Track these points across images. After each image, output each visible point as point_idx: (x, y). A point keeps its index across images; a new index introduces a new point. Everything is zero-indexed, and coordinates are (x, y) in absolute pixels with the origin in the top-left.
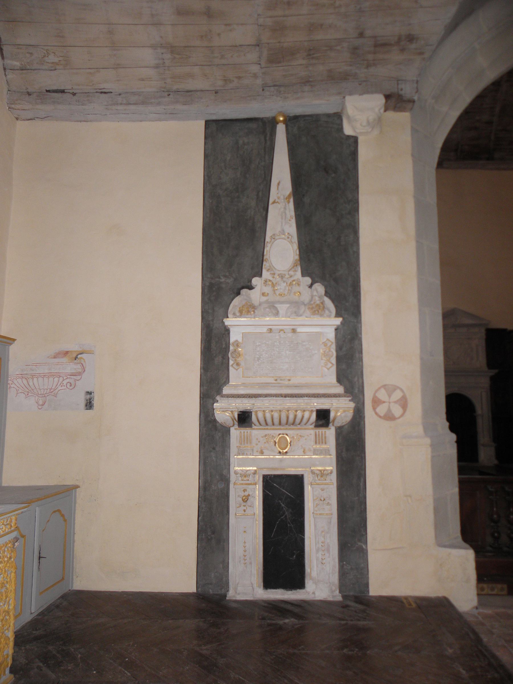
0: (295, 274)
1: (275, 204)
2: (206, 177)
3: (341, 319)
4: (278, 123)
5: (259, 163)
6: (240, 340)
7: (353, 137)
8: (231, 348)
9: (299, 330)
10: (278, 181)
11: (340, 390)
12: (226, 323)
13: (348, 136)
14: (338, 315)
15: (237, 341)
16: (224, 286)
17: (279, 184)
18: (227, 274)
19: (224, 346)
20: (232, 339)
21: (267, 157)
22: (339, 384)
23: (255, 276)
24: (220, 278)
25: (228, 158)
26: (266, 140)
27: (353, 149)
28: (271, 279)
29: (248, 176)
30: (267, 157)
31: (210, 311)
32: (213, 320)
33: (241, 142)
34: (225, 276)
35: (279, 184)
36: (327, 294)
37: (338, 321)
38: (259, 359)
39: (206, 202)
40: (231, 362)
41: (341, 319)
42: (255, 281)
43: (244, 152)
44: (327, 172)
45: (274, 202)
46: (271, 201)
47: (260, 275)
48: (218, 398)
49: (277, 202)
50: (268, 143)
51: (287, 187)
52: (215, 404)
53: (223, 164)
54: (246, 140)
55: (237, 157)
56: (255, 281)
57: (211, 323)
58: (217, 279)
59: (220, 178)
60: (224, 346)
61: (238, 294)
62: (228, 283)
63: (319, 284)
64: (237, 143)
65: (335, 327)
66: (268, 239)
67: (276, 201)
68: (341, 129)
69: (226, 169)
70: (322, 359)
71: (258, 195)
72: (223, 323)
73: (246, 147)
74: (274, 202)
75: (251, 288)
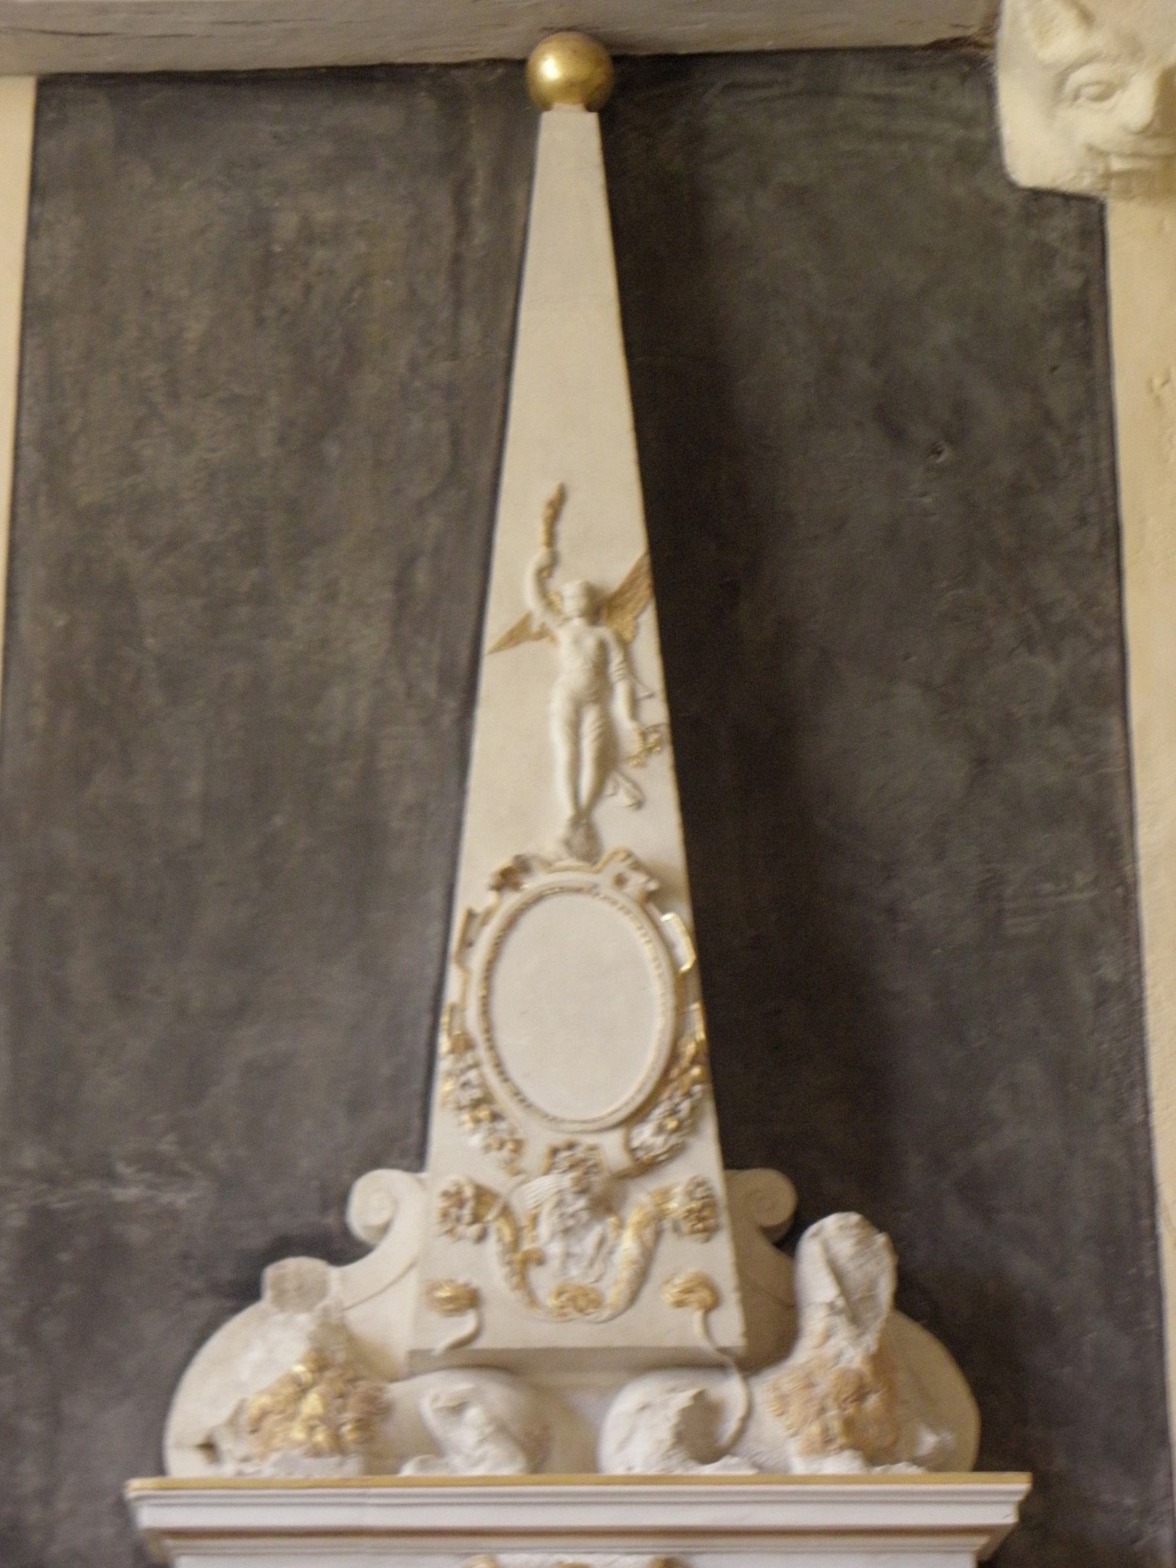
0: (675, 1152)
1: (526, 649)
2: (32, 457)
3: (1019, 1484)
4: (547, 107)
5: (414, 366)
7: (1068, 198)
10: (549, 491)
13: (1037, 194)
16: (137, 1234)
17: (556, 507)
18: (167, 1145)
21: (470, 327)
23: (376, 1163)
24: (111, 1177)
25: (195, 330)
26: (462, 217)
27: (1074, 280)
28: (493, 1176)
29: (333, 450)
30: (470, 327)
31: (32, 1426)
32: (46, 1496)
33: (287, 224)
34: (156, 1166)
35: (556, 507)
36: (911, 1297)
37: (995, 1501)
39: (25, 625)
41: (1019, 1484)
42: (375, 1198)
43: (308, 288)
44: (897, 435)
45: (518, 634)
46: (495, 626)
47: (413, 1154)
49: (544, 634)
50: (481, 232)
51: (614, 537)
53: (153, 370)
54: (324, 214)
55: (260, 322)
56: (375, 1198)
57: (34, 1514)
58: (92, 1186)
59: (134, 465)
61: (246, 1292)
62: (172, 1214)
63: (854, 1218)
64: (259, 227)
65: (981, 1541)
66: (474, 890)
67: (535, 628)
68: (982, 148)
69: (174, 396)
71: (401, 583)
72: (123, 1510)
73: (320, 254)
74: (518, 634)
75: (342, 1248)
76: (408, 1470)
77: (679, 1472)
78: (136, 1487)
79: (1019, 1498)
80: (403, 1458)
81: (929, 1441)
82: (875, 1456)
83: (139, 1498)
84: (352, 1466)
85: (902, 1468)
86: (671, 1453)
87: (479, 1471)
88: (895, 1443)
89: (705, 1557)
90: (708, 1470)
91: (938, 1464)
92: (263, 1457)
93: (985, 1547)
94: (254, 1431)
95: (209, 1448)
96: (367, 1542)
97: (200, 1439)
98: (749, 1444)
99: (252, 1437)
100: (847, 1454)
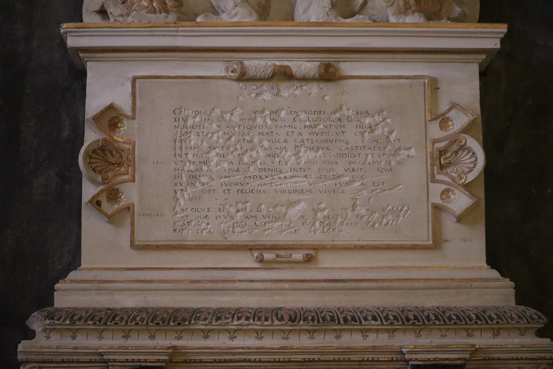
3: (503, 28)
6: (123, 102)
8: (91, 136)
9: (348, 68)
11: (497, 292)
12: (72, 42)
14: (486, 17)
15: (111, 107)
19: (66, 133)
20: (94, 103)
22: (495, 274)
37: (490, 37)
38: (193, 177)
40: (89, 191)
41: (503, 28)
48: (36, 322)
52: (20, 348)
60: (66, 133)
65: (484, 57)
70: (434, 181)
72: (63, 43)
76: (199, 20)
77: (334, 21)
78: (65, 27)
79: (502, 36)
80: (196, 16)
81: (457, 10)
82: (429, 17)
83: (66, 33)
84: (172, 17)
85: (444, 21)
86: (329, 13)
87: (235, 20)
88: (440, 10)
89: (345, 64)
90: (348, 21)
91: (461, 19)
92: (128, 15)
93: (484, 61)
94: (123, 3)
95: (103, 12)
96: (178, 54)
97: (97, 7)
98: (369, 8)
99: (122, 7)
100: (416, 14)
